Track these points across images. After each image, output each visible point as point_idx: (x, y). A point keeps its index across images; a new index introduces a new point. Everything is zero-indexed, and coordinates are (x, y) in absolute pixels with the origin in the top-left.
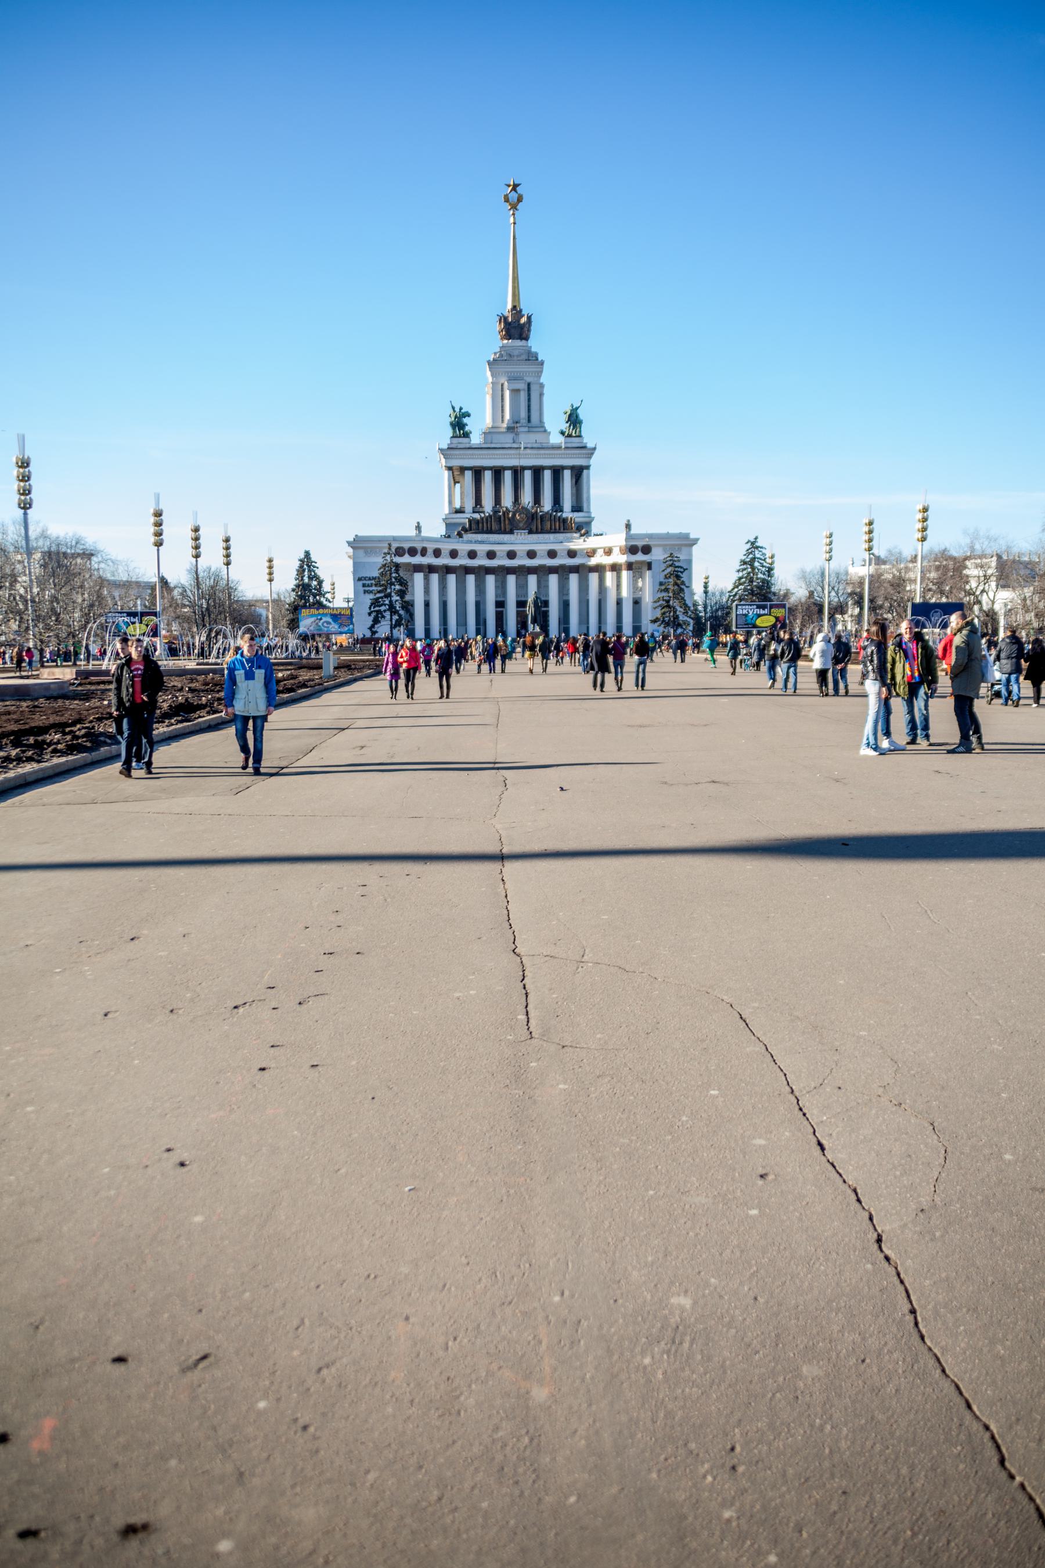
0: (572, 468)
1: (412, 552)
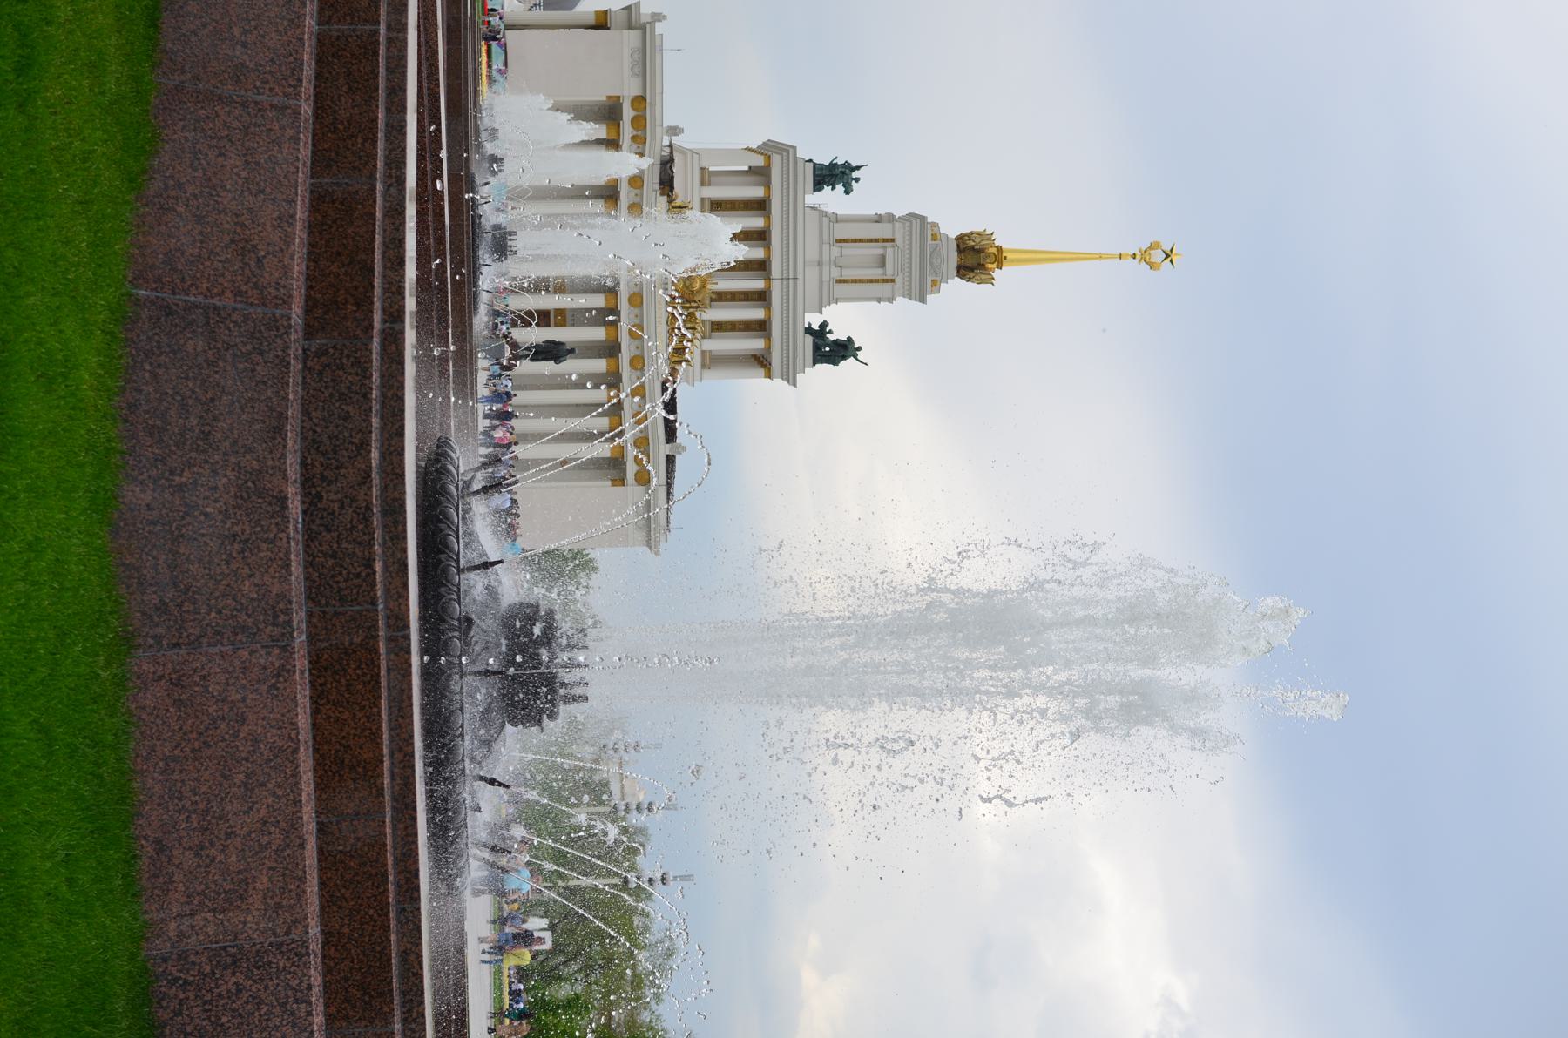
0: (768, 349)
1: (639, 122)
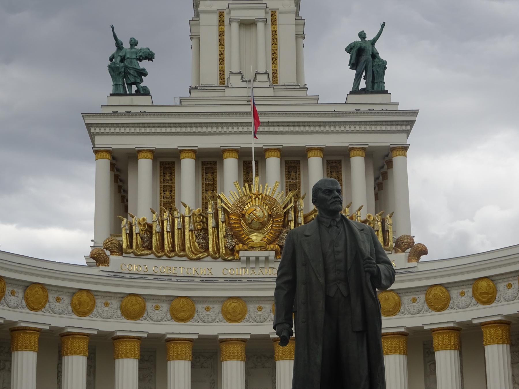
0: (369, 153)
